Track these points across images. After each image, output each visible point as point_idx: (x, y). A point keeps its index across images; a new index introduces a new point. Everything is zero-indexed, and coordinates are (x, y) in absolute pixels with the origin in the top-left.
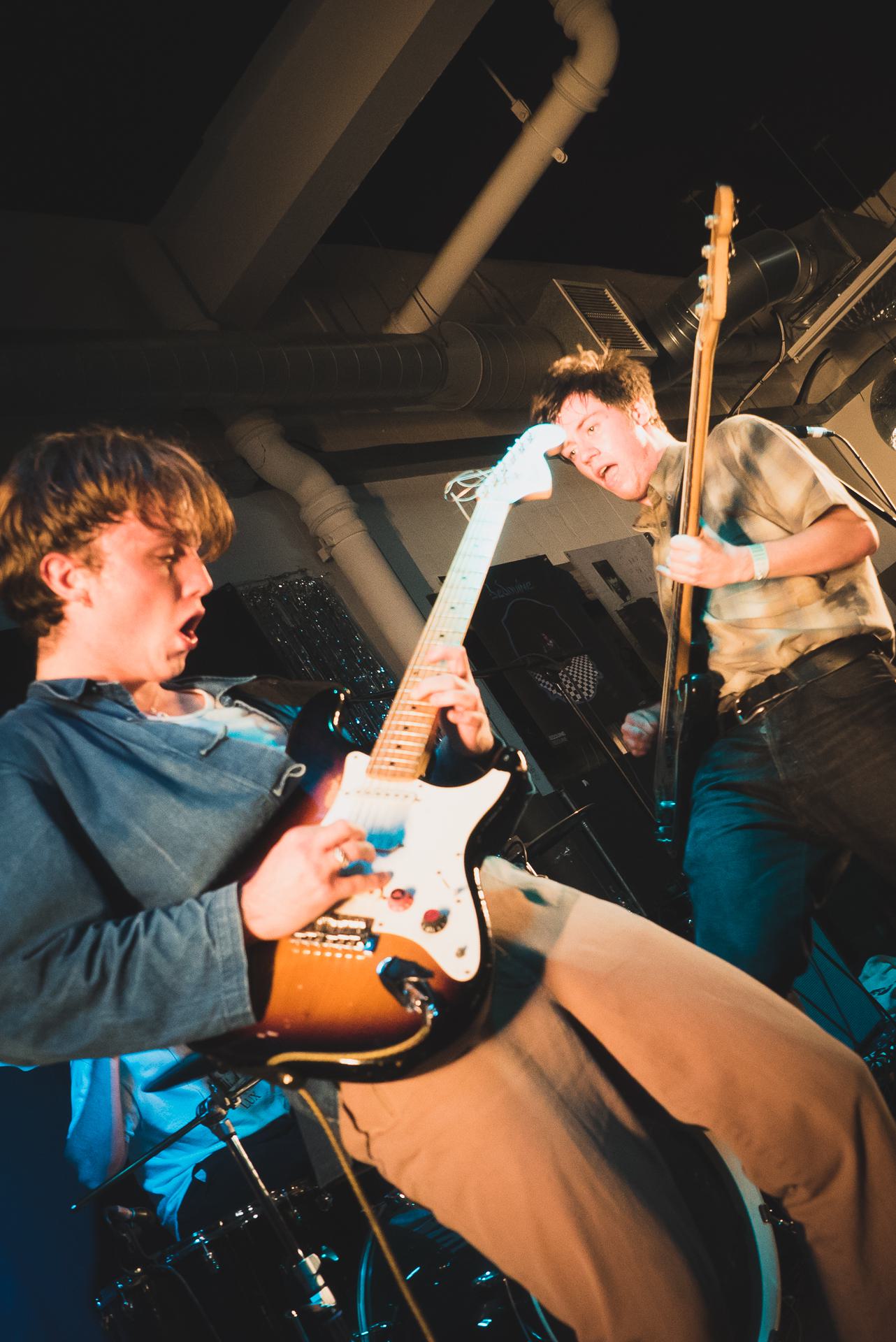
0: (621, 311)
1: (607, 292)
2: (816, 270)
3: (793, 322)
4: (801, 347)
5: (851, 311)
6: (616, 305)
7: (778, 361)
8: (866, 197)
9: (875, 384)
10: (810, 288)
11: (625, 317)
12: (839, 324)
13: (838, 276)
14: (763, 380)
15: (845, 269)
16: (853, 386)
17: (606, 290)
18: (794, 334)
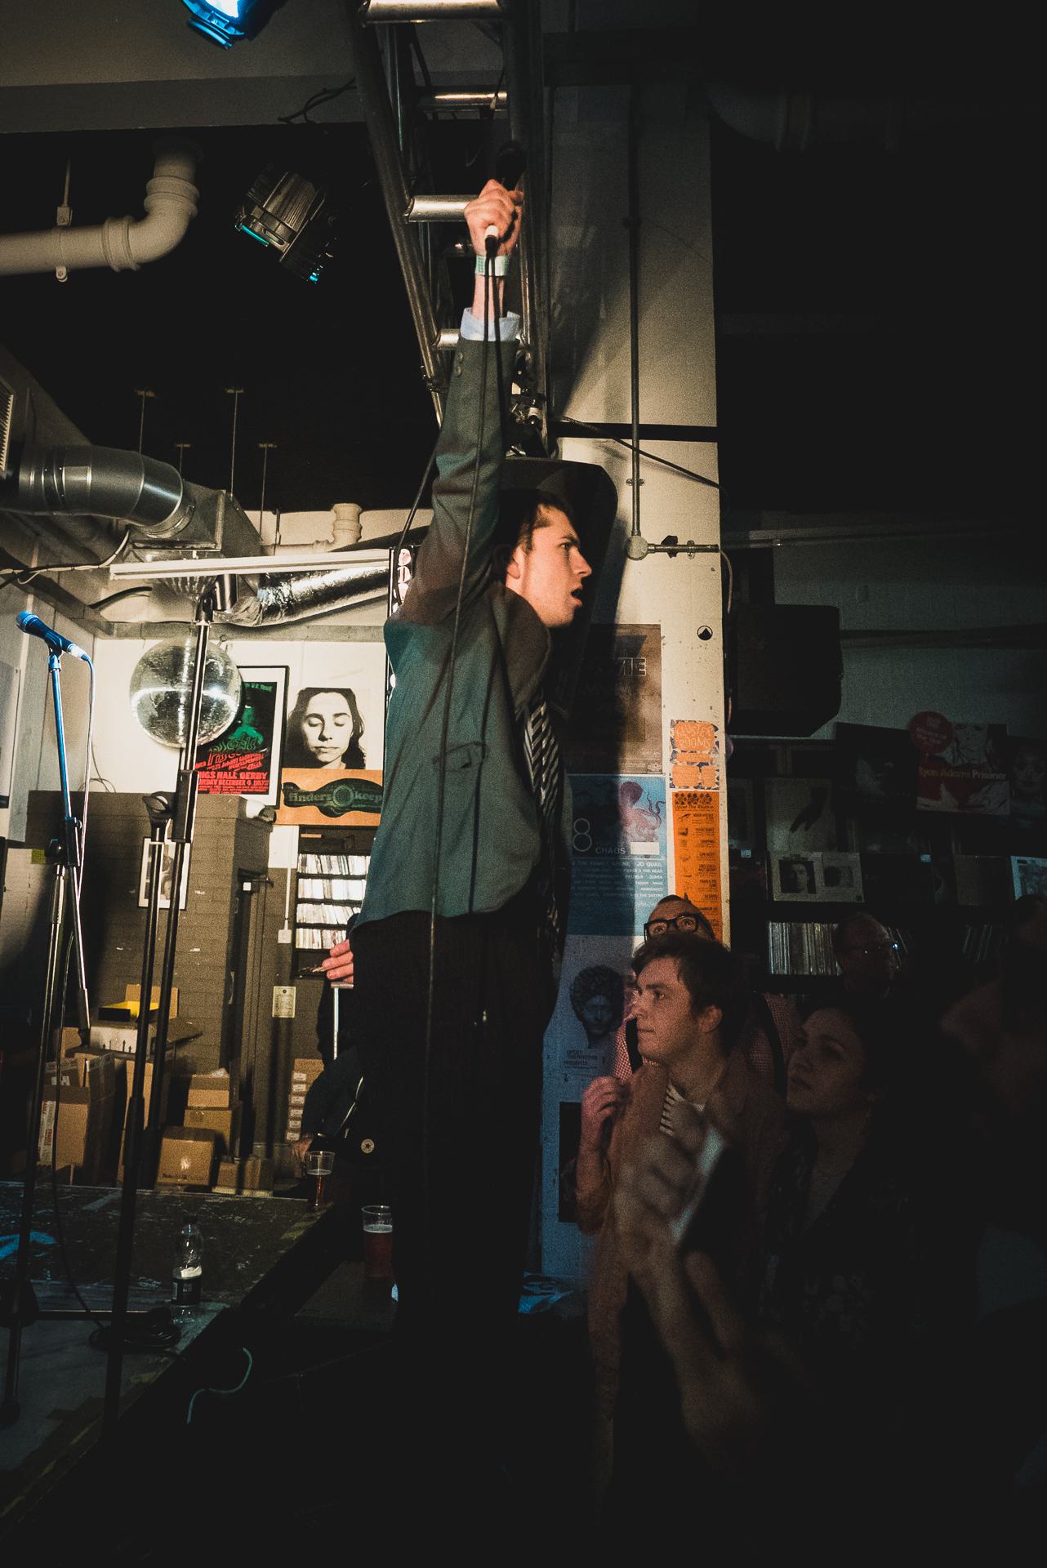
0: (9, 417)
1: (12, 398)
2: (182, 527)
3: (135, 547)
4: (126, 571)
5: (184, 579)
6: (10, 414)
7: (98, 565)
8: (266, 509)
9: (159, 645)
10: (167, 536)
11: (8, 429)
12: (169, 580)
13: (195, 546)
14: (76, 568)
15: (205, 545)
16: (147, 629)
17: (12, 396)
18: (129, 557)
